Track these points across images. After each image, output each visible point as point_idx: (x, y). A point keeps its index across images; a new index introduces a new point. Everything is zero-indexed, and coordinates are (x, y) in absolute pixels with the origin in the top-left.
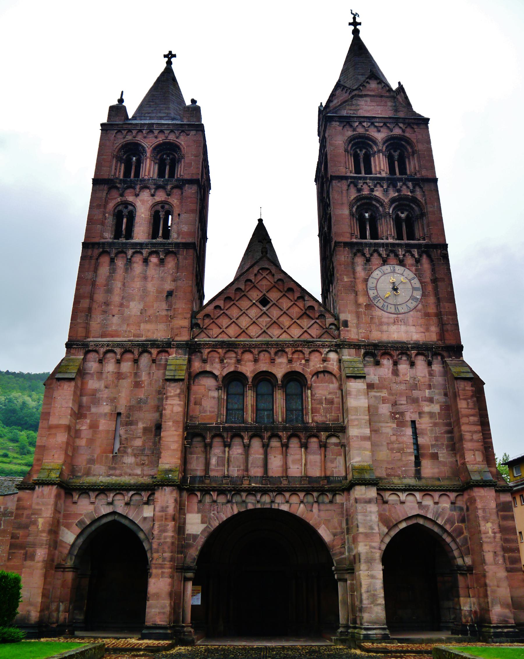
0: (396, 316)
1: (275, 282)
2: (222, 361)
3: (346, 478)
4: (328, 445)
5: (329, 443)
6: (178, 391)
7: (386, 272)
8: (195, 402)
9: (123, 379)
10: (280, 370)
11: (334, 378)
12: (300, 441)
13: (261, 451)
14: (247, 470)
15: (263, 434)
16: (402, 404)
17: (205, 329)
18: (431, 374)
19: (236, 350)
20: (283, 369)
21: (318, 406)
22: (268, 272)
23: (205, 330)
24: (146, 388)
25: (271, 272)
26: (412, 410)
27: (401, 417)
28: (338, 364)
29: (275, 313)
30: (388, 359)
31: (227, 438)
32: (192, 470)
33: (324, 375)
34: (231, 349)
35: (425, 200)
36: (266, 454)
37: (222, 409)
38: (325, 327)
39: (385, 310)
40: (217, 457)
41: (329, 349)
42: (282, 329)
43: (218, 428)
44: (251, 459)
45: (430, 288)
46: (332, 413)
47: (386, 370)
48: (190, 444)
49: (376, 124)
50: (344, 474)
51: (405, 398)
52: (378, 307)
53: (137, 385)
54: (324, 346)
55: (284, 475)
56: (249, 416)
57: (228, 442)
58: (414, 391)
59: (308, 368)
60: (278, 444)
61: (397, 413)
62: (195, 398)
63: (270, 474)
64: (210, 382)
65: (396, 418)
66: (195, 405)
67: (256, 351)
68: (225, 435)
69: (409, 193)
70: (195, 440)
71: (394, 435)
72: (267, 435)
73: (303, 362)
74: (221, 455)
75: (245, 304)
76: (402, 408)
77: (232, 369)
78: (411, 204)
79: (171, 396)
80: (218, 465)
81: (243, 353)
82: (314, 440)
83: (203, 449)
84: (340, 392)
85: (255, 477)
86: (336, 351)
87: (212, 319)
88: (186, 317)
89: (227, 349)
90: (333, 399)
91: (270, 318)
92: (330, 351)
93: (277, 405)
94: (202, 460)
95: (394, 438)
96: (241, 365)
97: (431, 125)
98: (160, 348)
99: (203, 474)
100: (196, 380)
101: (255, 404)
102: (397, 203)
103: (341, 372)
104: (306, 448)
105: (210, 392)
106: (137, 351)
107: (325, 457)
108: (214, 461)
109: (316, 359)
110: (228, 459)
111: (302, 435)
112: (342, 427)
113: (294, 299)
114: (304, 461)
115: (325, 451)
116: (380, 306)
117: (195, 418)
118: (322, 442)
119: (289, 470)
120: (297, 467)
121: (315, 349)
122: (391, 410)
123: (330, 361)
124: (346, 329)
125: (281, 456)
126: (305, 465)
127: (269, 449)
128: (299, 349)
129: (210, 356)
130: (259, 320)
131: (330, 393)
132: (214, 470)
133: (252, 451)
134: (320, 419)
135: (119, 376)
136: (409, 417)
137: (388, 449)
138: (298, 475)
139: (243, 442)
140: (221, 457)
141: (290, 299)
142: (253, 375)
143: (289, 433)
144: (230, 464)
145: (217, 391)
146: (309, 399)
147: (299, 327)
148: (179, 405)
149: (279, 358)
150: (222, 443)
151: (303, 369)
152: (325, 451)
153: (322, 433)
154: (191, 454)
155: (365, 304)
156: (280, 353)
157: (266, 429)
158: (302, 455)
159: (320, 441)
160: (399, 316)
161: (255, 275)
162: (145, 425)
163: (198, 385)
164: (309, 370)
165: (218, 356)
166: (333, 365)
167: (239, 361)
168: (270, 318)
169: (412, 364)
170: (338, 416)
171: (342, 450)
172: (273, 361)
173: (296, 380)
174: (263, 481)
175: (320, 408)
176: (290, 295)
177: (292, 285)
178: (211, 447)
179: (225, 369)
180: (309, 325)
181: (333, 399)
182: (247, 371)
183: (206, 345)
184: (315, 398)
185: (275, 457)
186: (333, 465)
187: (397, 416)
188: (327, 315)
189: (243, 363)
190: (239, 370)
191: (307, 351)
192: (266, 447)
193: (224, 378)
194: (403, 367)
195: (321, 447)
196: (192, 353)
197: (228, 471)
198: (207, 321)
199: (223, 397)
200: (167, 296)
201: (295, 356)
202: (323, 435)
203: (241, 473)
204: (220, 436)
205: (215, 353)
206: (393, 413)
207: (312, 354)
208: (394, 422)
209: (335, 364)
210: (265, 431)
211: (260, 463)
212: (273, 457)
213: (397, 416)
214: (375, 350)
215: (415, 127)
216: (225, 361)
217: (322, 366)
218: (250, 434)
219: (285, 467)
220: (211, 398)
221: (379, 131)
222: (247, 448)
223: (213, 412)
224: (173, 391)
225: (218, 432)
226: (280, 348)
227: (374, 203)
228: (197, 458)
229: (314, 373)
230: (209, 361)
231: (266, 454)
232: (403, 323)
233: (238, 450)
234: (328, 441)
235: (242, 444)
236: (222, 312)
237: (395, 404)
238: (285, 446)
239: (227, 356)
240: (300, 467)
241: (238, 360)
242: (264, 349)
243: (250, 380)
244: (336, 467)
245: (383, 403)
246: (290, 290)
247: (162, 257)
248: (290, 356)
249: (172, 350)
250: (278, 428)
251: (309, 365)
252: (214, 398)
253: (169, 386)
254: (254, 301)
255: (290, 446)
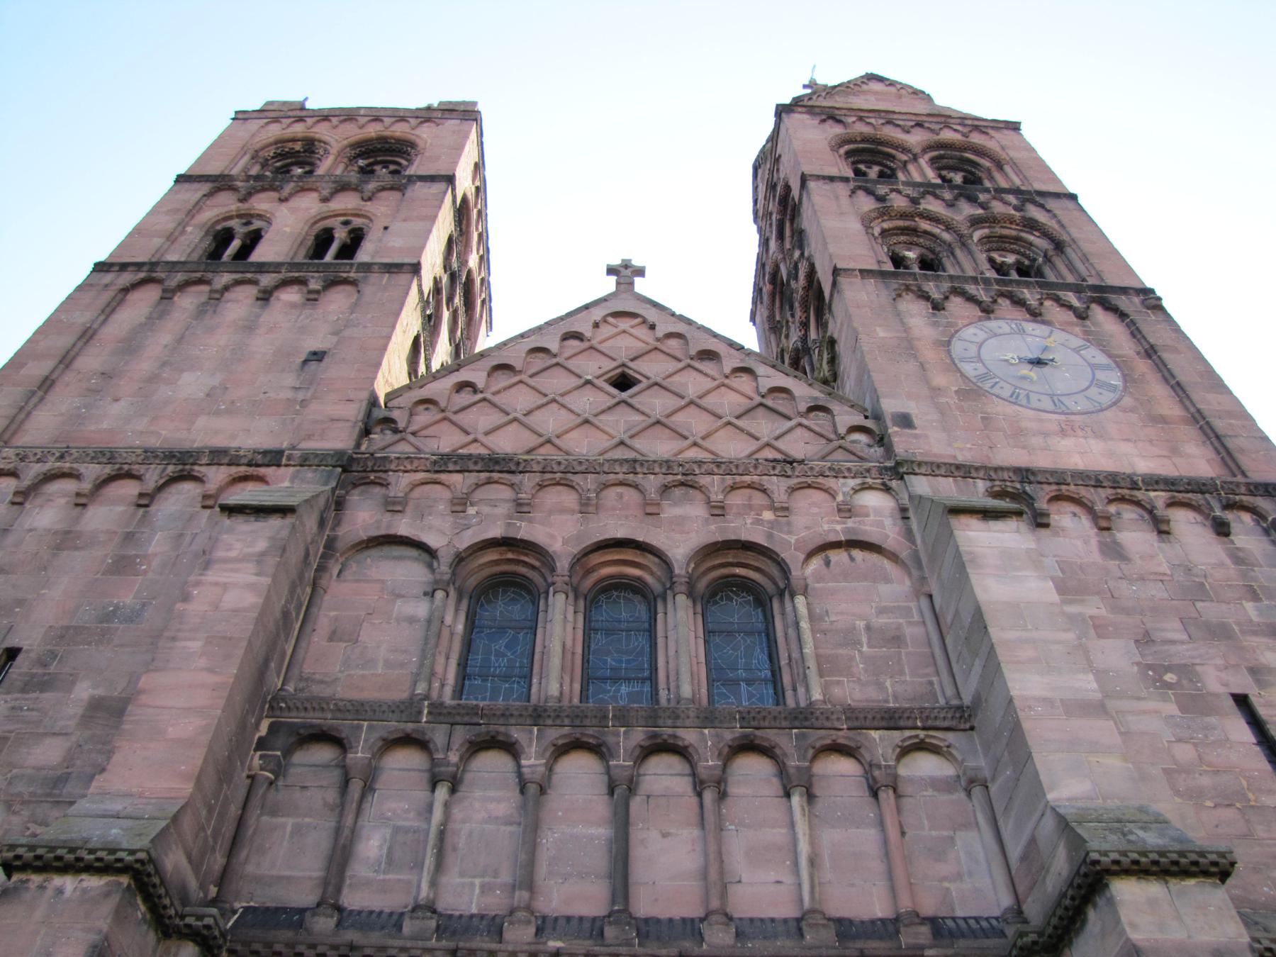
0: (1063, 417)
1: (658, 340)
2: (460, 504)
3: (1018, 912)
4: (904, 788)
5: (910, 780)
6: (261, 545)
7: (1001, 331)
8: (334, 632)
9: (76, 548)
10: (682, 532)
11: (887, 564)
12: (782, 772)
13: (601, 806)
14: (527, 881)
15: (611, 740)
16: (1173, 642)
17: (414, 434)
18: (1239, 558)
19: (516, 479)
20: (693, 535)
21: (840, 651)
22: (639, 320)
23: (411, 438)
24: (150, 575)
25: (644, 321)
26: (1219, 661)
27: (1185, 682)
28: (900, 522)
29: (657, 403)
30: (1075, 515)
31: (448, 748)
32: (258, 880)
33: (852, 559)
34: (496, 476)
35: (1059, 222)
36: (622, 824)
37: (441, 660)
38: (832, 436)
39: (1024, 402)
40: (387, 832)
41: (859, 481)
42: (686, 438)
43: (409, 708)
44: (549, 840)
45: (1143, 366)
46: (901, 672)
47: (1079, 543)
48: (279, 770)
49: (901, 123)
50: (1006, 901)
51: (1177, 624)
52: (997, 396)
53: (123, 565)
54: (840, 471)
55: (715, 904)
56: (555, 680)
57: (448, 764)
58: (1199, 605)
59: (789, 533)
60: (683, 785)
61: (1169, 669)
62: (336, 619)
63: (643, 906)
64: (407, 572)
65: (1168, 686)
66: (330, 639)
67: (590, 482)
68: (438, 736)
69: (1013, 212)
70: (300, 757)
71: (1179, 740)
72: (627, 740)
73: (768, 515)
74: (411, 822)
75: (556, 382)
76: (1184, 652)
77: (496, 532)
78: (1024, 235)
79: (226, 561)
80: (390, 861)
81: (541, 486)
82: (843, 766)
83: (332, 796)
84: (924, 602)
85: (569, 919)
86: (887, 489)
87: (443, 411)
88: (352, 397)
89: (484, 475)
90: (899, 627)
91: (643, 413)
92: (865, 487)
93: (672, 653)
94: (319, 841)
95: (1185, 753)
96: (530, 521)
97: (1024, 130)
98: (238, 465)
99: (303, 896)
100: (354, 567)
101: (579, 650)
102: (986, 231)
103: (913, 541)
104: (810, 797)
105: (399, 602)
106: (158, 471)
107: (903, 834)
108: (372, 845)
109: (815, 510)
110: (442, 834)
111: (785, 741)
112: (960, 708)
113: (722, 372)
114: (804, 847)
115: (899, 810)
116: (1006, 393)
117: (322, 682)
118: (879, 767)
119: (732, 889)
120: (773, 876)
121: (809, 480)
122: (1138, 659)
123: (868, 516)
124: (907, 431)
125: (696, 832)
126: (812, 863)
127: (636, 803)
128: (747, 478)
129: (417, 493)
130: (602, 417)
131: (882, 611)
132: (368, 883)
133: (557, 802)
134: (858, 695)
135: (65, 540)
136: (1219, 680)
137: (1178, 793)
138: (786, 910)
139: (519, 766)
140: (407, 831)
141: (706, 375)
142: (575, 550)
143: (728, 736)
144: (450, 859)
145: (427, 598)
146: (804, 625)
147: (745, 436)
148: (250, 587)
149: (675, 504)
150: (426, 776)
151: (770, 536)
152: (899, 810)
153: (875, 734)
154: (274, 813)
155: (954, 389)
156: (678, 492)
157: (623, 719)
158: (792, 825)
159: (869, 768)
160: (1073, 417)
161: (596, 325)
162: (100, 692)
163: (357, 581)
164: (793, 539)
165: (447, 494)
166: (880, 524)
167: (521, 508)
168: (643, 413)
169: (1161, 528)
170: (931, 683)
171: (977, 804)
172: (650, 511)
173: (743, 583)
174: (609, 932)
175: (852, 659)
176: (707, 366)
177: (712, 345)
178: (368, 789)
179: (469, 532)
180: (778, 433)
181: (899, 627)
182: (552, 537)
183: (407, 463)
184: (825, 625)
185: (665, 835)
186: (947, 868)
187: (1169, 677)
188: (835, 407)
189: (537, 515)
190: (521, 535)
191: (778, 486)
192: (622, 791)
193: (460, 559)
194: (1134, 535)
195: (875, 794)
196: (355, 486)
197: (433, 884)
198: (423, 417)
199: (449, 619)
200: (305, 362)
201: (737, 499)
202: (881, 743)
203: (495, 903)
204: (417, 742)
205: (438, 487)
206: (1150, 667)
207: (798, 494)
208: (1164, 698)
209: (888, 522)
210: (618, 725)
211: (598, 860)
212: (654, 835)
213: (1169, 677)
214: (1021, 482)
215: (991, 132)
216: (471, 511)
217: (838, 527)
218: (553, 734)
219: (716, 876)
220: (398, 620)
221: (908, 132)
222: (533, 791)
223: (402, 665)
224: (238, 545)
225: (410, 726)
226: (683, 479)
227: (925, 225)
228: (298, 831)
229: (811, 547)
230: (409, 509)
231: (622, 824)
232: (1090, 433)
233: (492, 806)
234: (903, 771)
235: (512, 779)
236: (480, 396)
237: (1145, 640)
238: (711, 787)
239: (479, 494)
240: (788, 879)
241: (520, 505)
242: (621, 476)
243: (563, 565)
244: (959, 877)
245: (1100, 636)
246: (708, 355)
247: (314, 285)
248: (717, 496)
249: (282, 470)
250: (675, 715)
251: (789, 524)
252: (412, 620)
253: (230, 530)
254: (589, 377)
255: (733, 790)
